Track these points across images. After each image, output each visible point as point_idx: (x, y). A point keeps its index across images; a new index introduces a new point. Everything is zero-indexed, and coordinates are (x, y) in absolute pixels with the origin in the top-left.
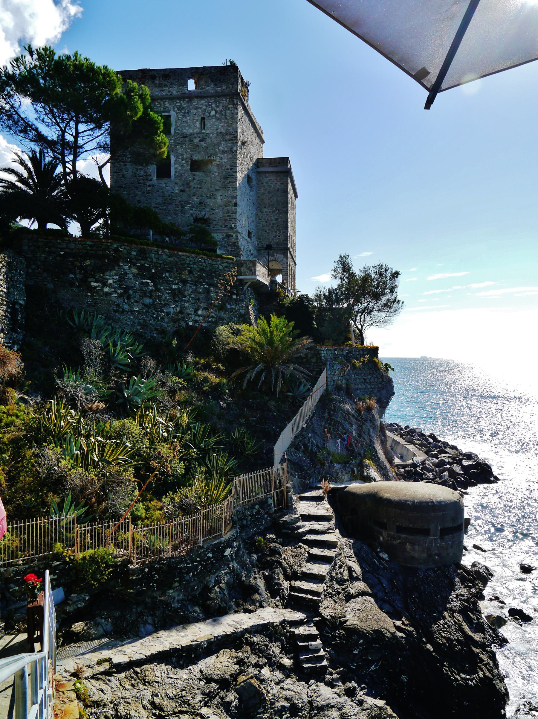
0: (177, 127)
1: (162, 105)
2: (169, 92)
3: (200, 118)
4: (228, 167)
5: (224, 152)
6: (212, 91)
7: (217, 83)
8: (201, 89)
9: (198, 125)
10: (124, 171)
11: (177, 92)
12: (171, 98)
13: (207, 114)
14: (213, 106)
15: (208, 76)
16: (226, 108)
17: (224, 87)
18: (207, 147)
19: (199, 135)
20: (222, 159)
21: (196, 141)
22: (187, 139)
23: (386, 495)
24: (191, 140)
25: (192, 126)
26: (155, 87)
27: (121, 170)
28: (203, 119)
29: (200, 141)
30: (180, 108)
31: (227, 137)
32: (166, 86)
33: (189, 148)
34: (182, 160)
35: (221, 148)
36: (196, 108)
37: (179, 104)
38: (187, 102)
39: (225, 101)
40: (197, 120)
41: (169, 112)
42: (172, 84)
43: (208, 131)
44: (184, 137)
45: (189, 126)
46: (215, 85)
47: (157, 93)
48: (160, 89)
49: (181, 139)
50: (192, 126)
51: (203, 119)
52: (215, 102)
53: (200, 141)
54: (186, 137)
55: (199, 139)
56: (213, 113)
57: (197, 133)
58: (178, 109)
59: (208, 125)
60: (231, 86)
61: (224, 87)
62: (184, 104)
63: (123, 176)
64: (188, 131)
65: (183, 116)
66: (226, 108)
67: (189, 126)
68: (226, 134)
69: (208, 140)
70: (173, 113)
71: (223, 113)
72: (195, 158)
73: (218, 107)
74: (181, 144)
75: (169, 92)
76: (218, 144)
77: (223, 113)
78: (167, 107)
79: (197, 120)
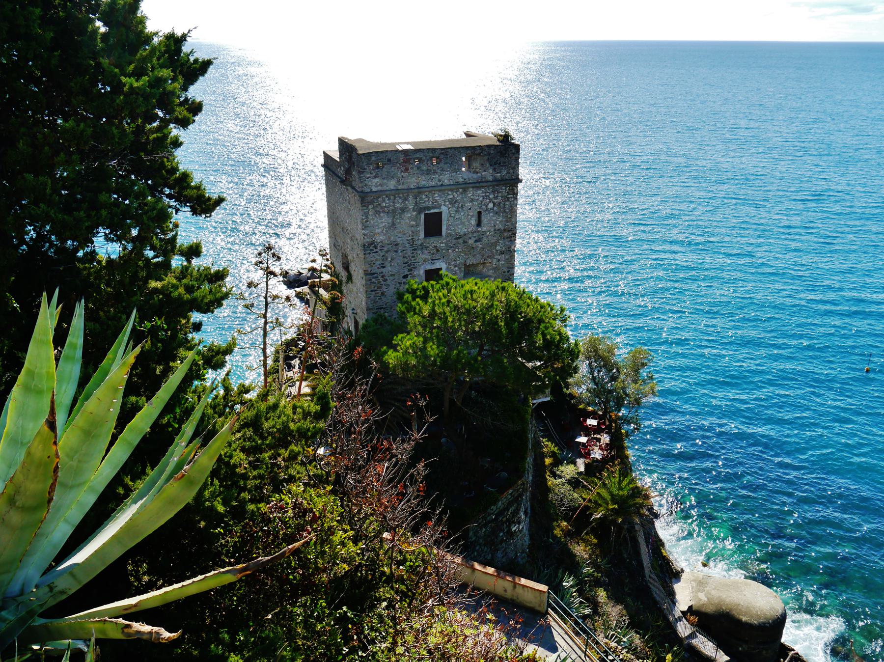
0: (448, 226)
1: (431, 199)
2: (439, 181)
3: (476, 213)
4: (506, 270)
5: (502, 253)
6: (490, 178)
7: (496, 166)
8: (474, 172)
9: (473, 222)
10: (384, 287)
11: (449, 181)
12: (441, 188)
13: (484, 207)
14: (491, 196)
15: (486, 157)
16: (506, 199)
17: (504, 173)
18: (483, 249)
19: (475, 235)
20: (499, 261)
21: (471, 242)
22: (461, 241)
23: (744, 619)
24: (465, 242)
25: (467, 223)
26: (422, 175)
27: (380, 287)
28: (479, 213)
29: (476, 241)
30: (453, 202)
31: (506, 234)
32: (435, 172)
33: (462, 252)
34: (455, 266)
35: (498, 248)
36: (472, 201)
37: (451, 197)
38: (461, 193)
39: (504, 190)
40: (472, 216)
41: (440, 207)
42: (443, 170)
43: (484, 229)
44: (457, 239)
45: (462, 224)
46: (494, 170)
47: (424, 183)
48: (429, 177)
49: (454, 241)
50: (467, 223)
51: (479, 213)
52: (494, 192)
53: (476, 241)
54: (459, 238)
55: (474, 239)
56: (491, 205)
57: (472, 233)
58: (451, 203)
59: (485, 220)
60: (512, 171)
61: (504, 173)
62: (457, 196)
63: (383, 294)
64: (461, 230)
65: (456, 211)
66: (506, 199)
67: (462, 224)
68: (505, 230)
69: (485, 239)
70: (444, 209)
71: (502, 205)
72: (469, 262)
73: (496, 198)
74: (453, 247)
75: (439, 181)
76: (495, 244)
77: (502, 205)
78: (436, 201)
79: (472, 216)
